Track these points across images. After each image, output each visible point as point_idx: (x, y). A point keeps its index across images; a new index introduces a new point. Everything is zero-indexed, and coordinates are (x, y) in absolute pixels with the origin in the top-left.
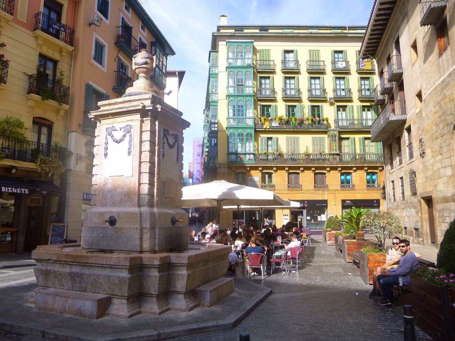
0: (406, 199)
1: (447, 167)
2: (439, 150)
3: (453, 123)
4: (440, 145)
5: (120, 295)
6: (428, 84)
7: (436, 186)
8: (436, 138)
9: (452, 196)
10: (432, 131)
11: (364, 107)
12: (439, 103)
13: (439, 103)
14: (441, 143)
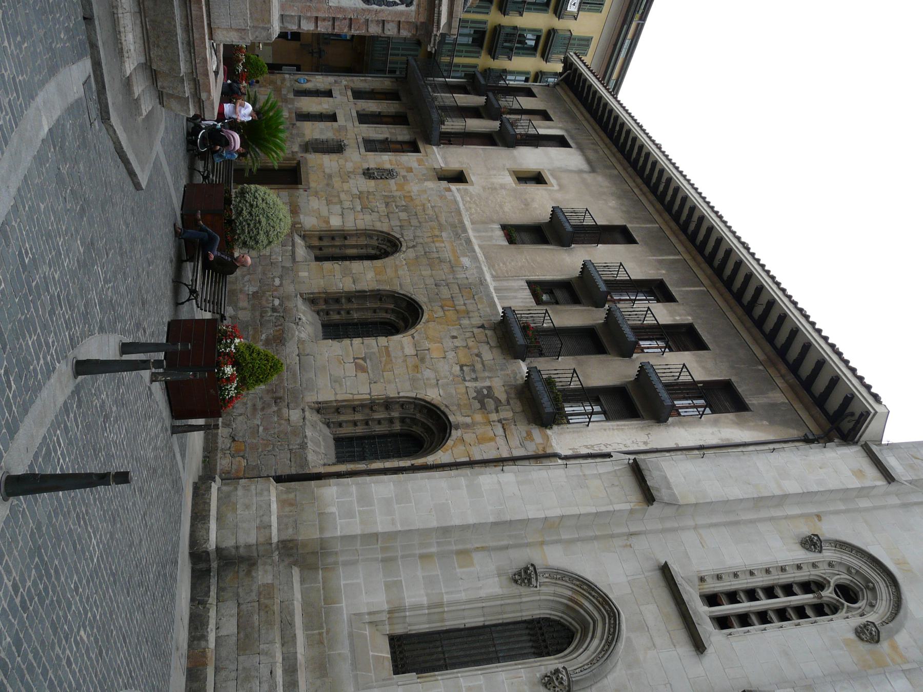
0: (298, 124)
1: (343, 218)
2: (369, 207)
3: (403, 237)
4: (376, 210)
5: (152, 56)
6: (471, 199)
7: (316, 194)
8: (388, 203)
9: (300, 223)
10: (400, 198)
11: (483, 33)
12: (437, 217)
13: (437, 217)
14: (378, 212)
